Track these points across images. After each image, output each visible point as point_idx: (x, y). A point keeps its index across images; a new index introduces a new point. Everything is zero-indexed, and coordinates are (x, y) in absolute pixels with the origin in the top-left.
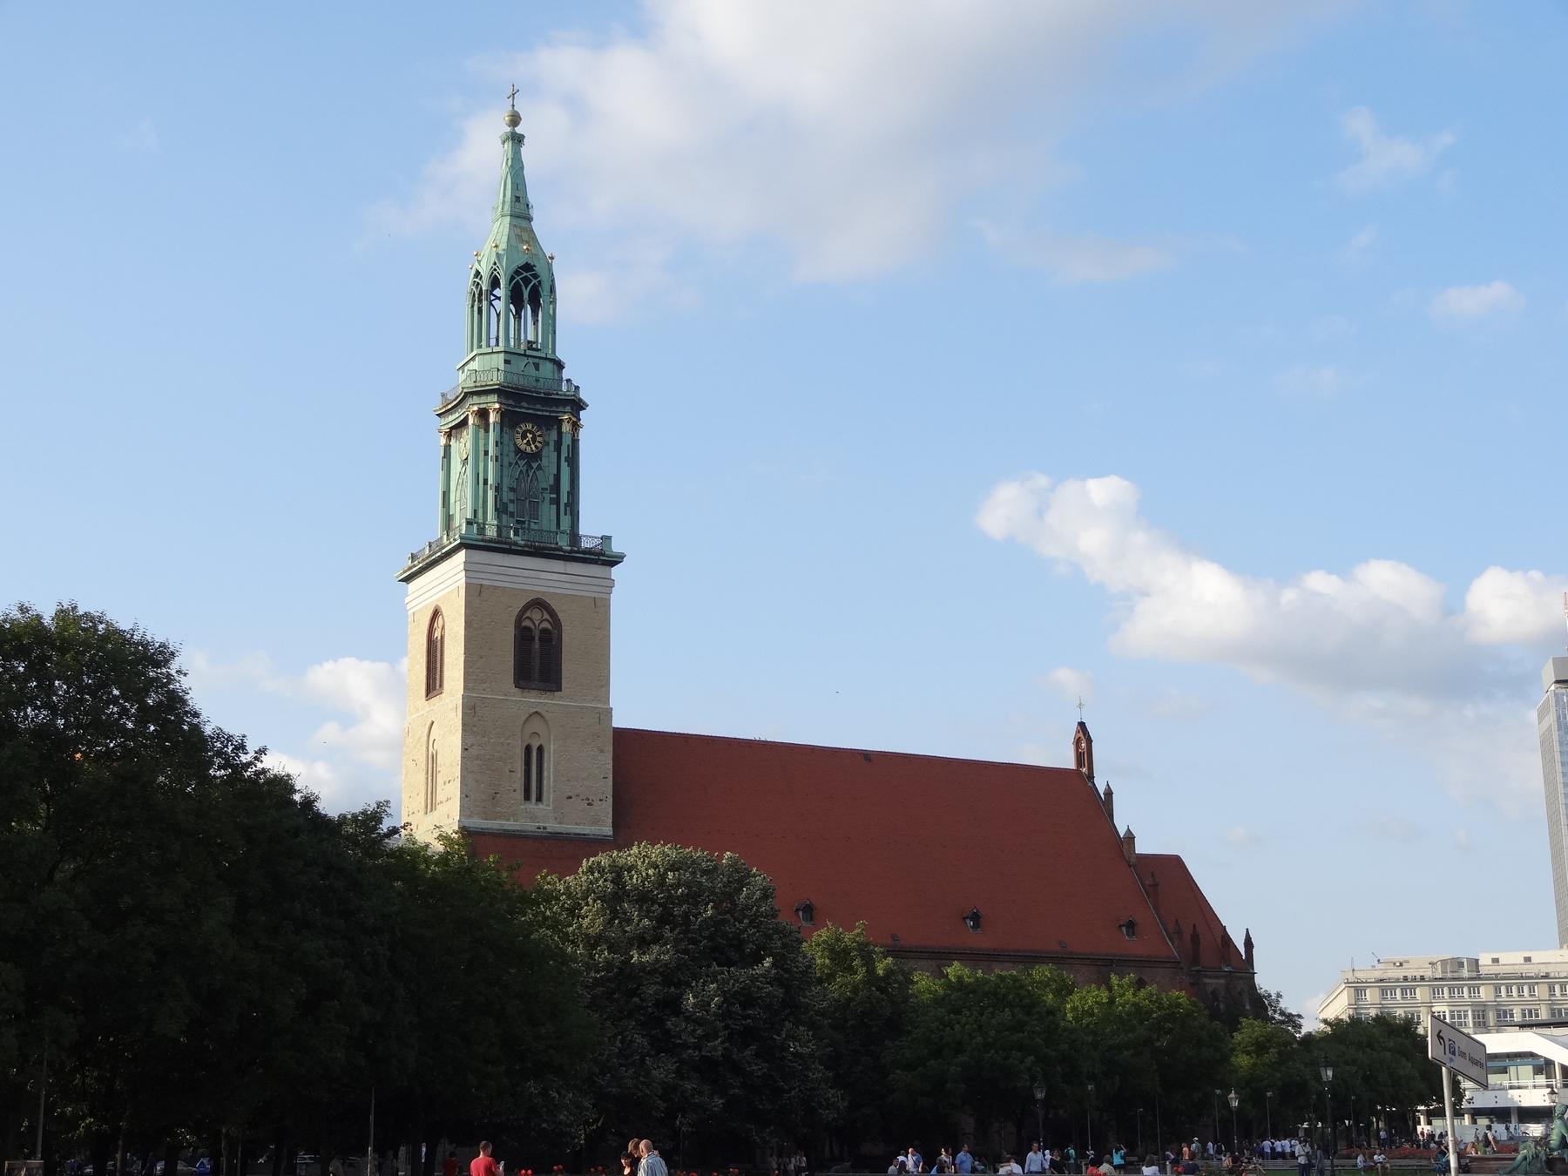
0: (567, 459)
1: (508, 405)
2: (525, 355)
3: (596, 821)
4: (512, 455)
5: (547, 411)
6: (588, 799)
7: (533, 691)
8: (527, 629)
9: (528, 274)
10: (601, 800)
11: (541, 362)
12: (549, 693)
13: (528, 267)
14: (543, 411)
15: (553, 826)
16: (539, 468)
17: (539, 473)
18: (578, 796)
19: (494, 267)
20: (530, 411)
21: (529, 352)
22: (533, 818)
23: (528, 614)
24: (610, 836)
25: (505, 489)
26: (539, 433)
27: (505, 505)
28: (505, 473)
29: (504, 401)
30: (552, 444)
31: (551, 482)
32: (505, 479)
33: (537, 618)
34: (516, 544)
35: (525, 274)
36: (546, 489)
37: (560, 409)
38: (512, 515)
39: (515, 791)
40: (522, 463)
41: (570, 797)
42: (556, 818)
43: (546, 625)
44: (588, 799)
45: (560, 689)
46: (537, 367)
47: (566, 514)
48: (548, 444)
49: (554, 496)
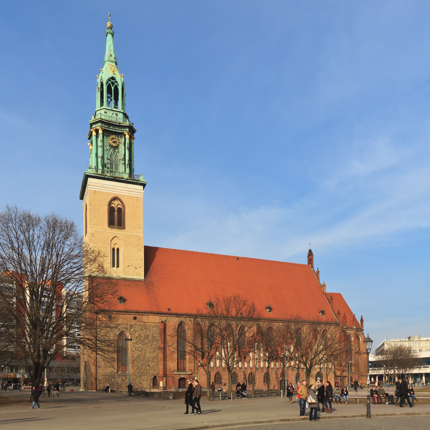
2: (112, 110)
3: (138, 274)
6: (135, 267)
7: (115, 229)
8: (113, 208)
9: (113, 81)
10: (140, 267)
11: (118, 113)
12: (121, 230)
13: (113, 78)
15: (122, 276)
16: (118, 152)
17: (118, 154)
18: (131, 265)
19: (102, 78)
20: (114, 130)
21: (113, 109)
22: (116, 273)
23: (113, 202)
24: (143, 279)
30: (123, 144)
31: (123, 157)
33: (116, 204)
34: (106, 176)
35: (112, 81)
37: (125, 130)
39: (109, 263)
41: (129, 266)
42: (124, 273)
43: (119, 206)
44: (135, 267)
45: (124, 228)
46: (117, 115)
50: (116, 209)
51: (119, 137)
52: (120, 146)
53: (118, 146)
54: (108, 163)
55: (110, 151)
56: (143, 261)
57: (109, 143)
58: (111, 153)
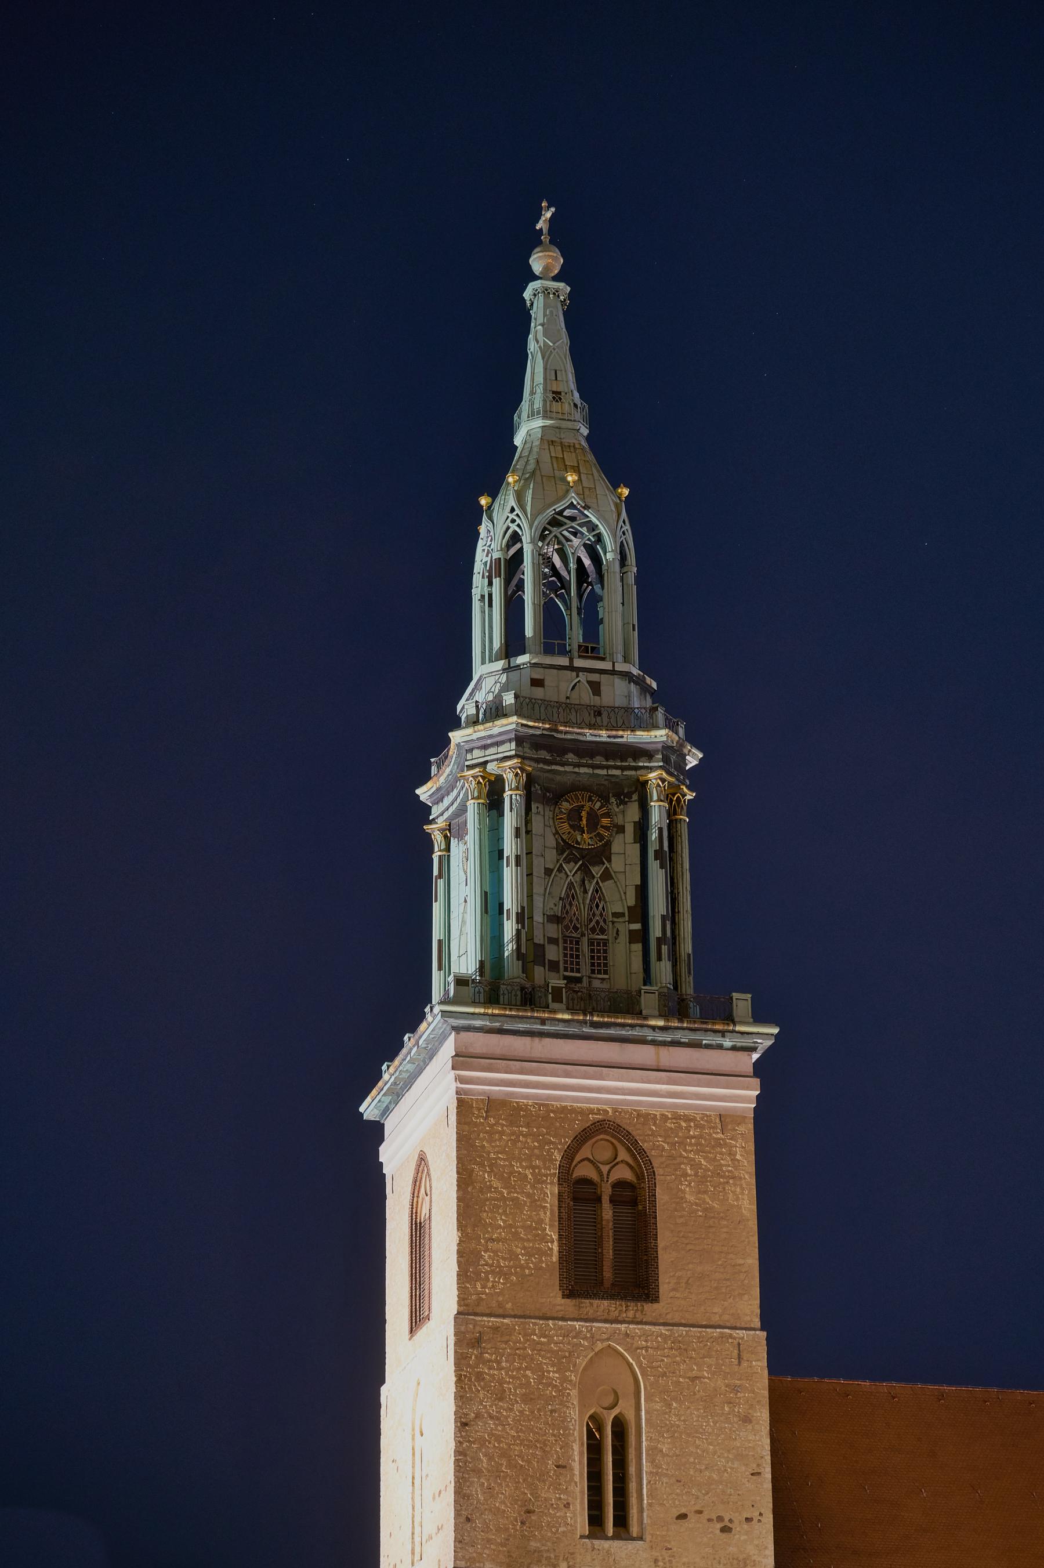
0: (659, 854)
1: (538, 761)
4: (551, 855)
5: (617, 768)
6: (720, 1519)
11: (604, 679)
14: (608, 767)
16: (607, 876)
17: (607, 887)
18: (700, 1512)
21: (578, 663)
23: (585, 1152)
25: (538, 918)
26: (604, 810)
27: (540, 949)
28: (538, 889)
29: (530, 753)
30: (630, 829)
31: (631, 901)
32: (538, 901)
36: (622, 915)
38: (554, 966)
40: (571, 868)
41: (683, 1517)
47: (659, 959)
48: (621, 829)
49: (637, 926)
50: (606, 1192)
51: (613, 800)
52: (616, 847)
53: (608, 844)
54: (553, 941)
55: (563, 875)
56: (768, 1486)
57: (557, 833)
58: (571, 886)
